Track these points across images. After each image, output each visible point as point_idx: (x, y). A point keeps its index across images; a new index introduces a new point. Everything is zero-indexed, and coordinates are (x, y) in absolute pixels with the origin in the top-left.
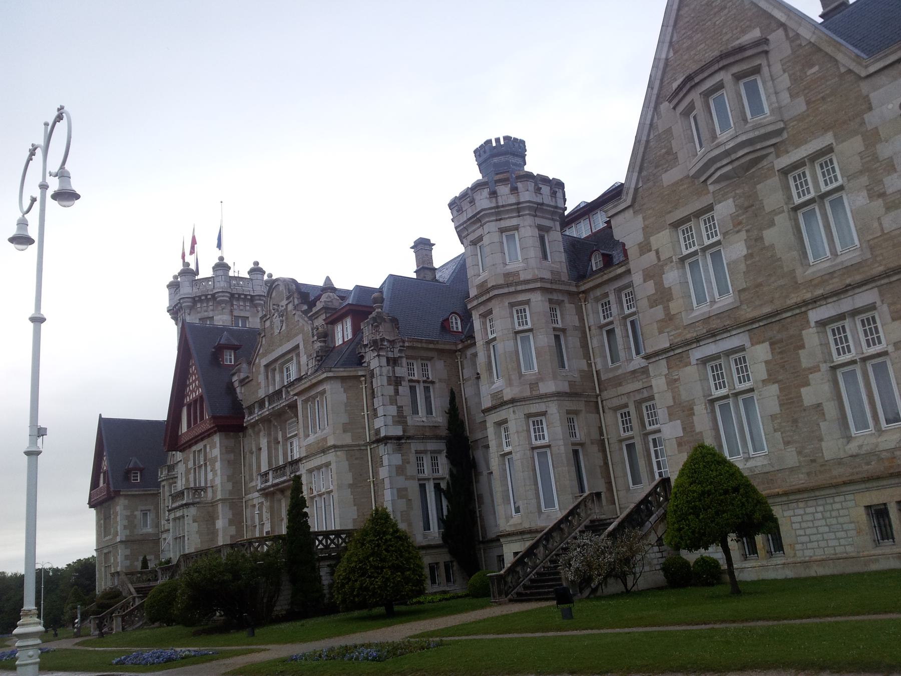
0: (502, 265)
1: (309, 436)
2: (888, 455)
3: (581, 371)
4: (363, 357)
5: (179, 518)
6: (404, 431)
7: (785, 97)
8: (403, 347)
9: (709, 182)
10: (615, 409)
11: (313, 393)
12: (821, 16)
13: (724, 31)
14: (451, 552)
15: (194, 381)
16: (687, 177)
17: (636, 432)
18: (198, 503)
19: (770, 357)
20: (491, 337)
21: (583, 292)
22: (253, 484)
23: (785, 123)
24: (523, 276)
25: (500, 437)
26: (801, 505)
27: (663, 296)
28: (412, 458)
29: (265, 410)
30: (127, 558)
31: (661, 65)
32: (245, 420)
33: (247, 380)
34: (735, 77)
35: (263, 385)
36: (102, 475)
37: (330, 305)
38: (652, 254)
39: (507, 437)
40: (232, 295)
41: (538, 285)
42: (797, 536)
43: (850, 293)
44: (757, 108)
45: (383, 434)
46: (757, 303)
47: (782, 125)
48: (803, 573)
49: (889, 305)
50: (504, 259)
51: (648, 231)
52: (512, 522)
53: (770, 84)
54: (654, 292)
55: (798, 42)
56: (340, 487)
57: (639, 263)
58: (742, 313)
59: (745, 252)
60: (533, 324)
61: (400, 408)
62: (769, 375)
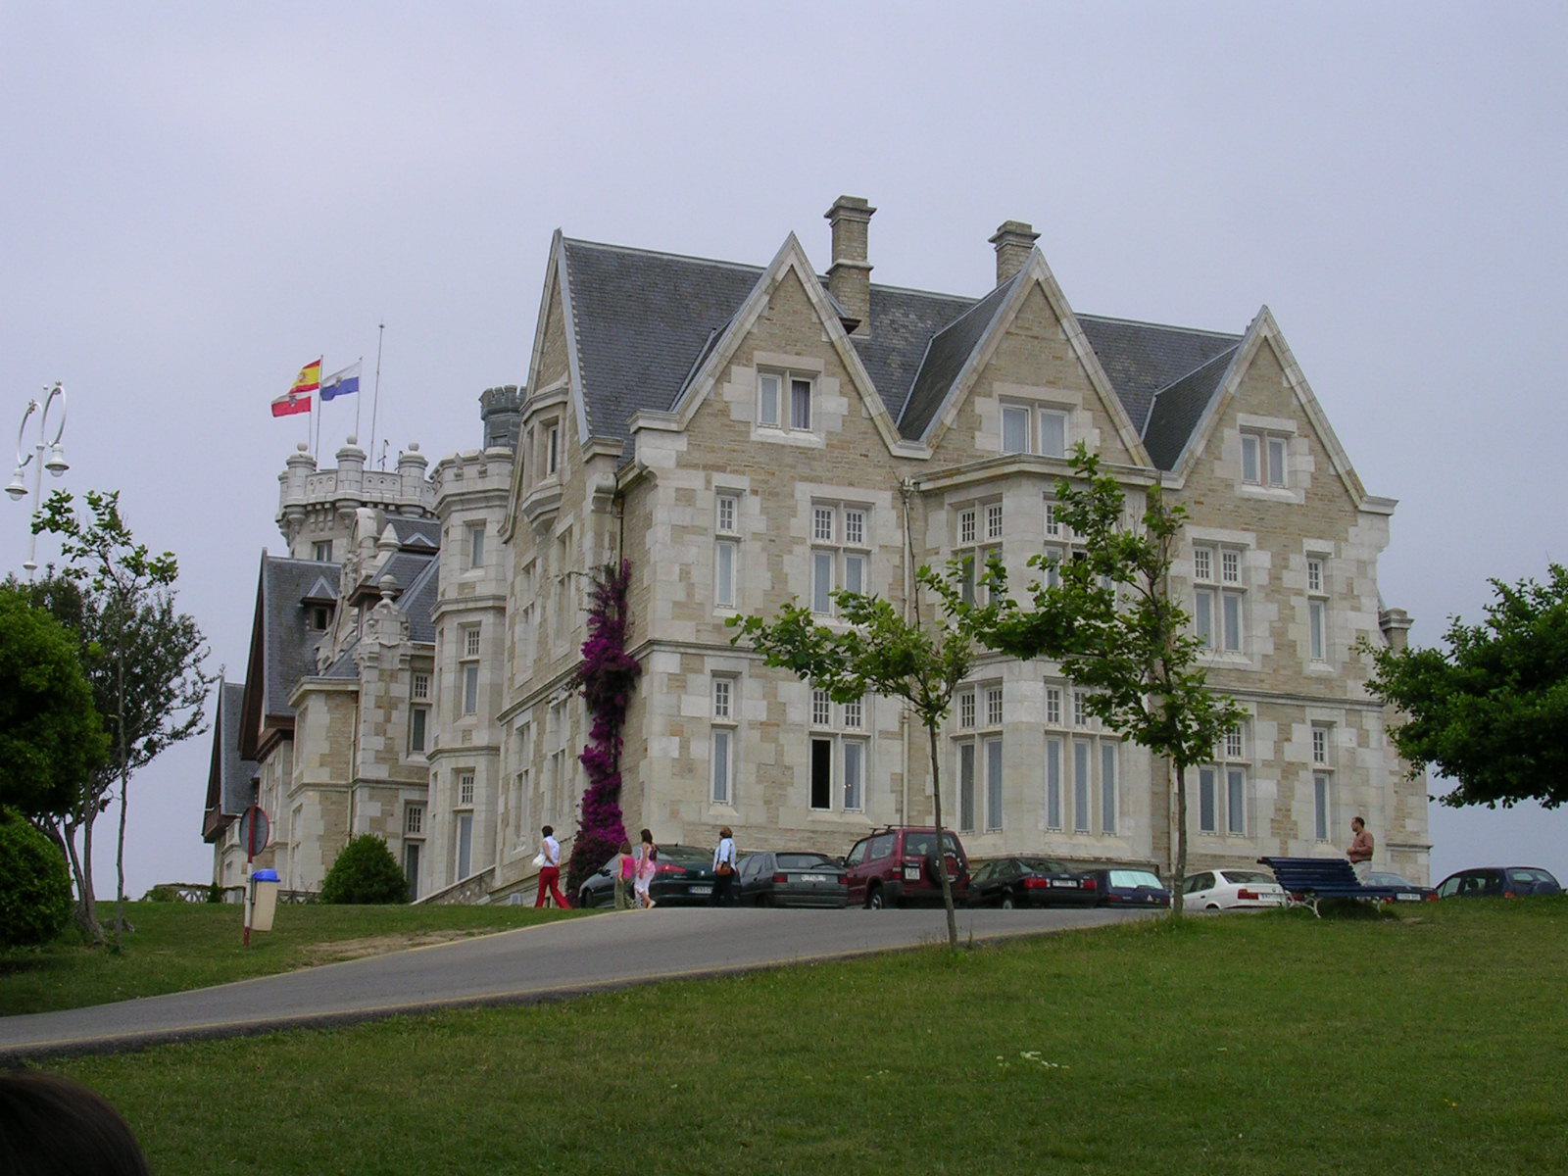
28: (399, 809)
34: (544, 425)
41: (490, 603)
47: (557, 490)
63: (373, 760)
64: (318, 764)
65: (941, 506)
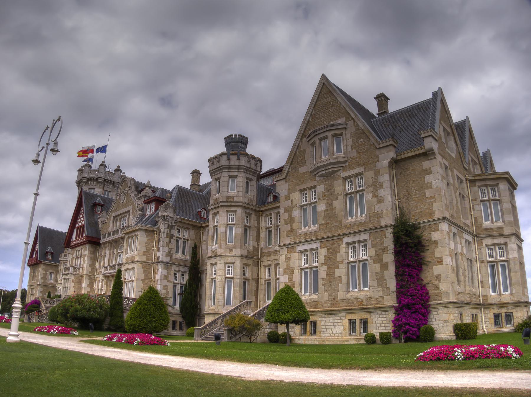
0: (227, 192)
1: (127, 254)
2: (360, 300)
3: (254, 247)
4: (157, 222)
5: (66, 279)
6: (170, 260)
7: (350, 148)
8: (177, 221)
9: (317, 176)
10: (266, 266)
11: (132, 235)
12: (377, 114)
13: (332, 115)
14: (183, 317)
15: (81, 218)
16: (309, 171)
17: (272, 278)
18: (76, 274)
19: (326, 255)
20: (216, 224)
21: (262, 211)
22: (100, 270)
23: (348, 158)
24: (235, 199)
25: (212, 270)
26: (326, 316)
27: (291, 221)
28: (172, 272)
29: (111, 237)
30: (41, 292)
31: (306, 122)
32: (101, 240)
33: (105, 222)
35: (111, 225)
36: (35, 252)
37: (147, 195)
38: (290, 201)
39: (215, 271)
40: (105, 180)
41: (241, 204)
42: (322, 328)
43: (359, 234)
44: (339, 150)
45: (160, 259)
46: (326, 231)
47: (347, 160)
48: (321, 343)
49: (372, 241)
50: (228, 189)
51: (290, 191)
52: (211, 308)
53: (345, 141)
54: (288, 218)
55: (358, 127)
56: (137, 280)
57: (283, 204)
58: (320, 234)
59: (325, 208)
60: (236, 222)
61: (170, 249)
62: (325, 262)
63: (165, 256)
64: (142, 255)
65: (475, 186)
